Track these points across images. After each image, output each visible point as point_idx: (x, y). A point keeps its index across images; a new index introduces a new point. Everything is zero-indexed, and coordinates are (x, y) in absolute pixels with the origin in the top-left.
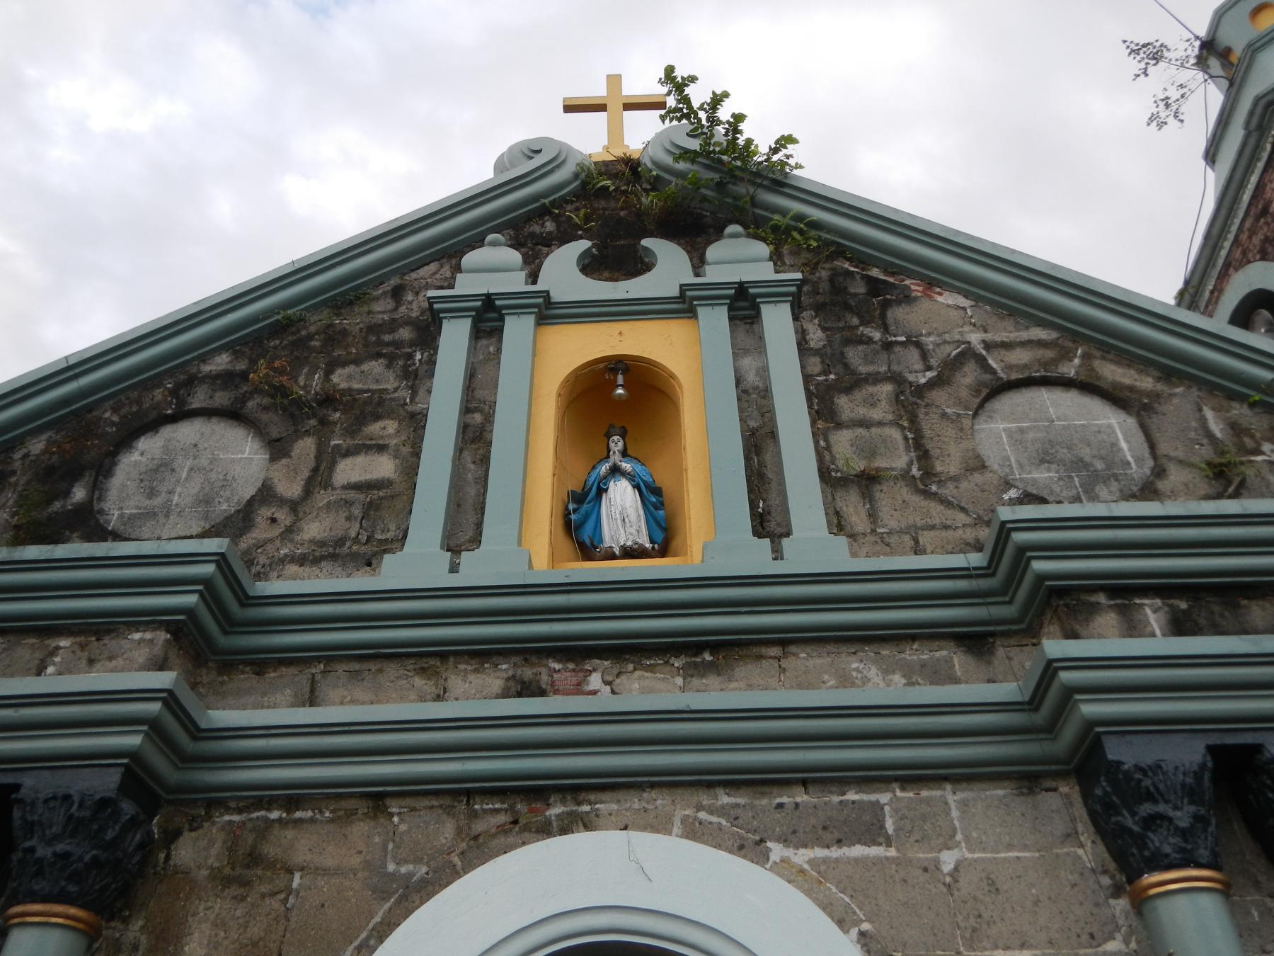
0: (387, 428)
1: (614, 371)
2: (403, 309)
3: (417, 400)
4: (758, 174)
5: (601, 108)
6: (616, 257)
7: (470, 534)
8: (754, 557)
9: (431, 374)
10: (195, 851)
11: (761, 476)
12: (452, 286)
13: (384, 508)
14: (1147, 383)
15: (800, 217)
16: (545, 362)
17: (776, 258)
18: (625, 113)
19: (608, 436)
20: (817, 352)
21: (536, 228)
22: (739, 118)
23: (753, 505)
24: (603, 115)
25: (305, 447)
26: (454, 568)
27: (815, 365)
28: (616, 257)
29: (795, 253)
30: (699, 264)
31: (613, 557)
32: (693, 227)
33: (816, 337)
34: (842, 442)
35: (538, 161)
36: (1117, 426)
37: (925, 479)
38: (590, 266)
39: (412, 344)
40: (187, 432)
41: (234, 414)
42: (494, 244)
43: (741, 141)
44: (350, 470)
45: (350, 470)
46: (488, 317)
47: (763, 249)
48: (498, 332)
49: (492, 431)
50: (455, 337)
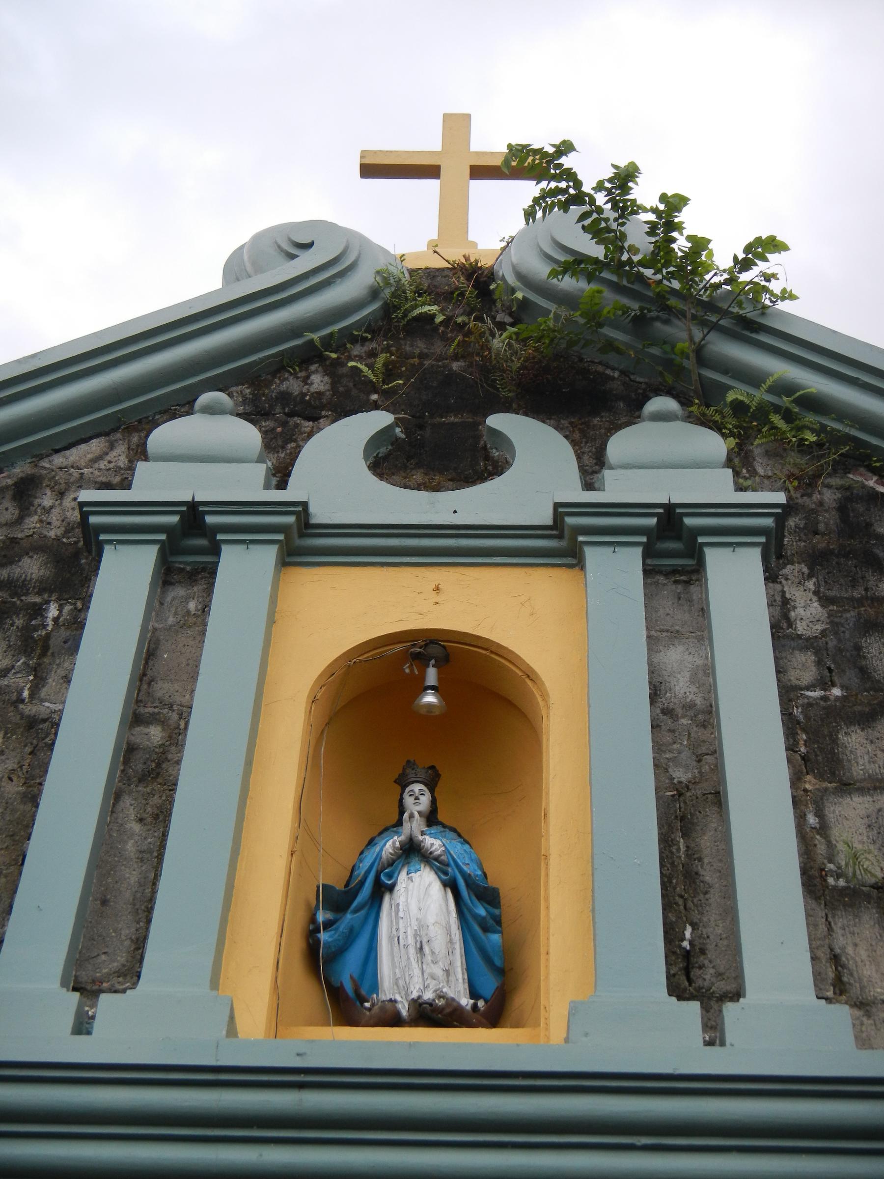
1: (421, 659)
2: (32, 522)
3: (43, 693)
4: (710, 306)
5: (430, 171)
6: (439, 444)
7: (122, 958)
8: (671, 1038)
9: (74, 649)
11: (691, 877)
12: (126, 485)
15: (785, 388)
16: (290, 636)
17: (739, 463)
18: (477, 186)
19: (403, 783)
20: (808, 644)
21: (293, 385)
22: (674, 204)
23: (671, 934)
24: (432, 186)
26: (83, 1026)
27: (804, 668)
28: (439, 444)
29: (775, 454)
30: (592, 466)
31: (393, 1020)
32: (585, 395)
33: (809, 614)
34: (850, 817)
35: (306, 262)
38: (389, 460)
39: (44, 587)
42: (211, 410)
43: (681, 244)
46: (190, 544)
47: (715, 445)
48: (207, 574)
49: (178, 762)
50: (125, 578)
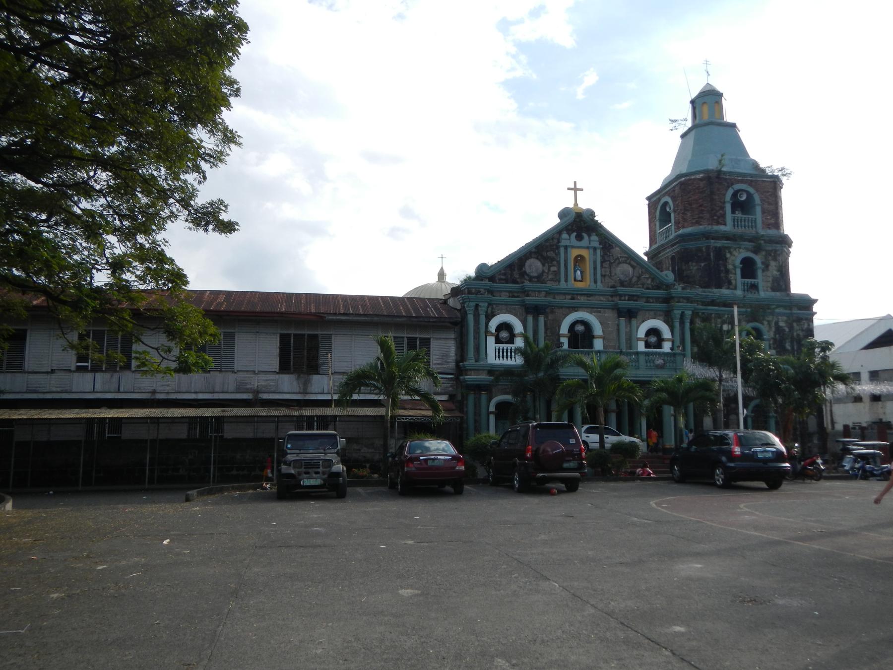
0: (555, 263)
6: (579, 238)
10: (548, 310)
13: (557, 273)
28: (579, 238)
36: (631, 269)
37: (610, 276)
41: (537, 258)
44: (553, 269)
45: (553, 269)
46: (566, 248)
50: (562, 250)
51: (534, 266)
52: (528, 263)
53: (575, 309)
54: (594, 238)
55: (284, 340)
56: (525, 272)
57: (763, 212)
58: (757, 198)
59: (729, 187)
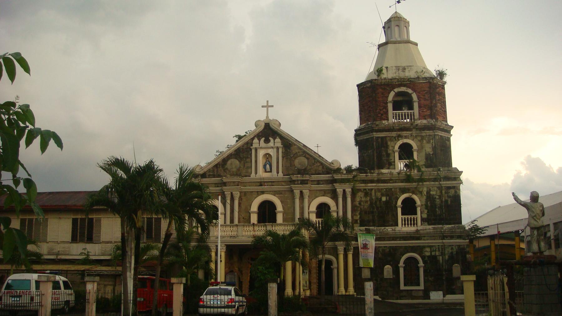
6: (267, 141)
14: (309, 157)
25: (242, 162)
28: (267, 141)
36: (306, 161)
40: (232, 160)
41: (236, 158)
46: (256, 150)
50: (253, 151)
51: (234, 163)
52: (229, 162)
53: (263, 193)
54: (278, 140)
55: (75, 221)
56: (227, 169)
57: (420, 107)
58: (415, 97)
59: (391, 91)
